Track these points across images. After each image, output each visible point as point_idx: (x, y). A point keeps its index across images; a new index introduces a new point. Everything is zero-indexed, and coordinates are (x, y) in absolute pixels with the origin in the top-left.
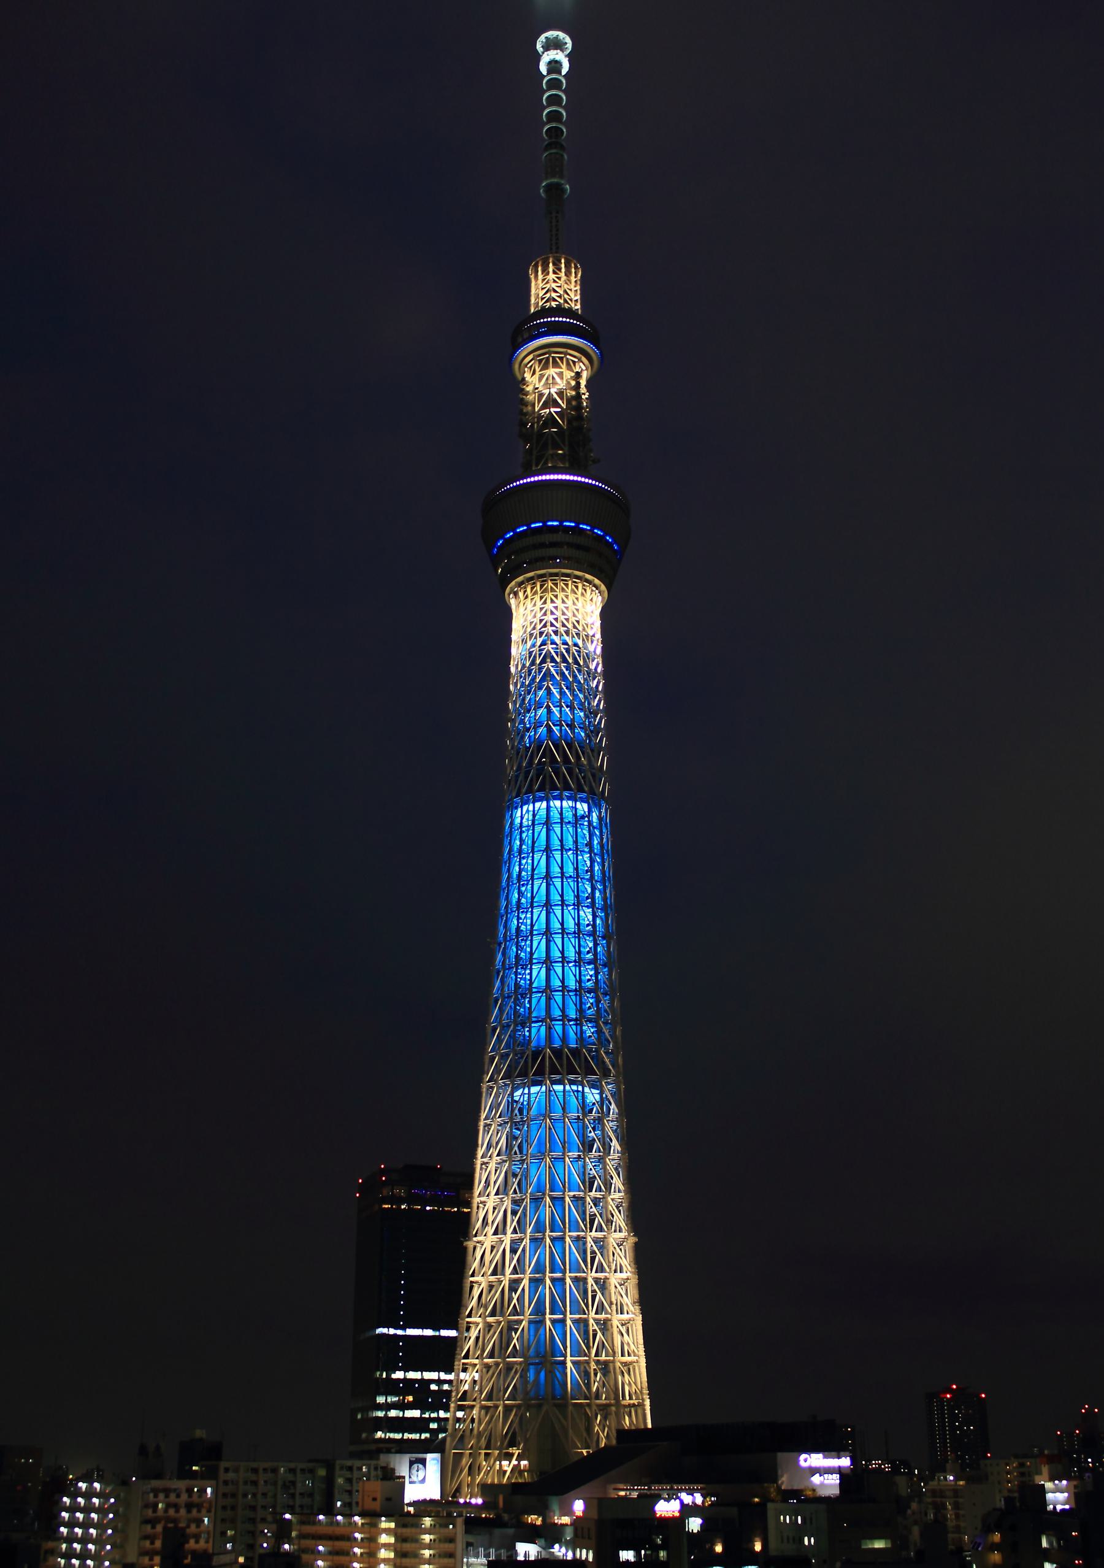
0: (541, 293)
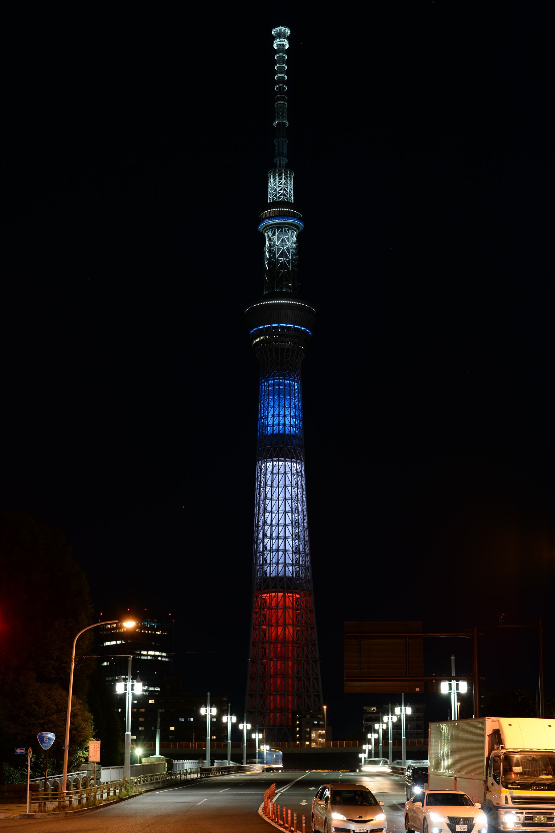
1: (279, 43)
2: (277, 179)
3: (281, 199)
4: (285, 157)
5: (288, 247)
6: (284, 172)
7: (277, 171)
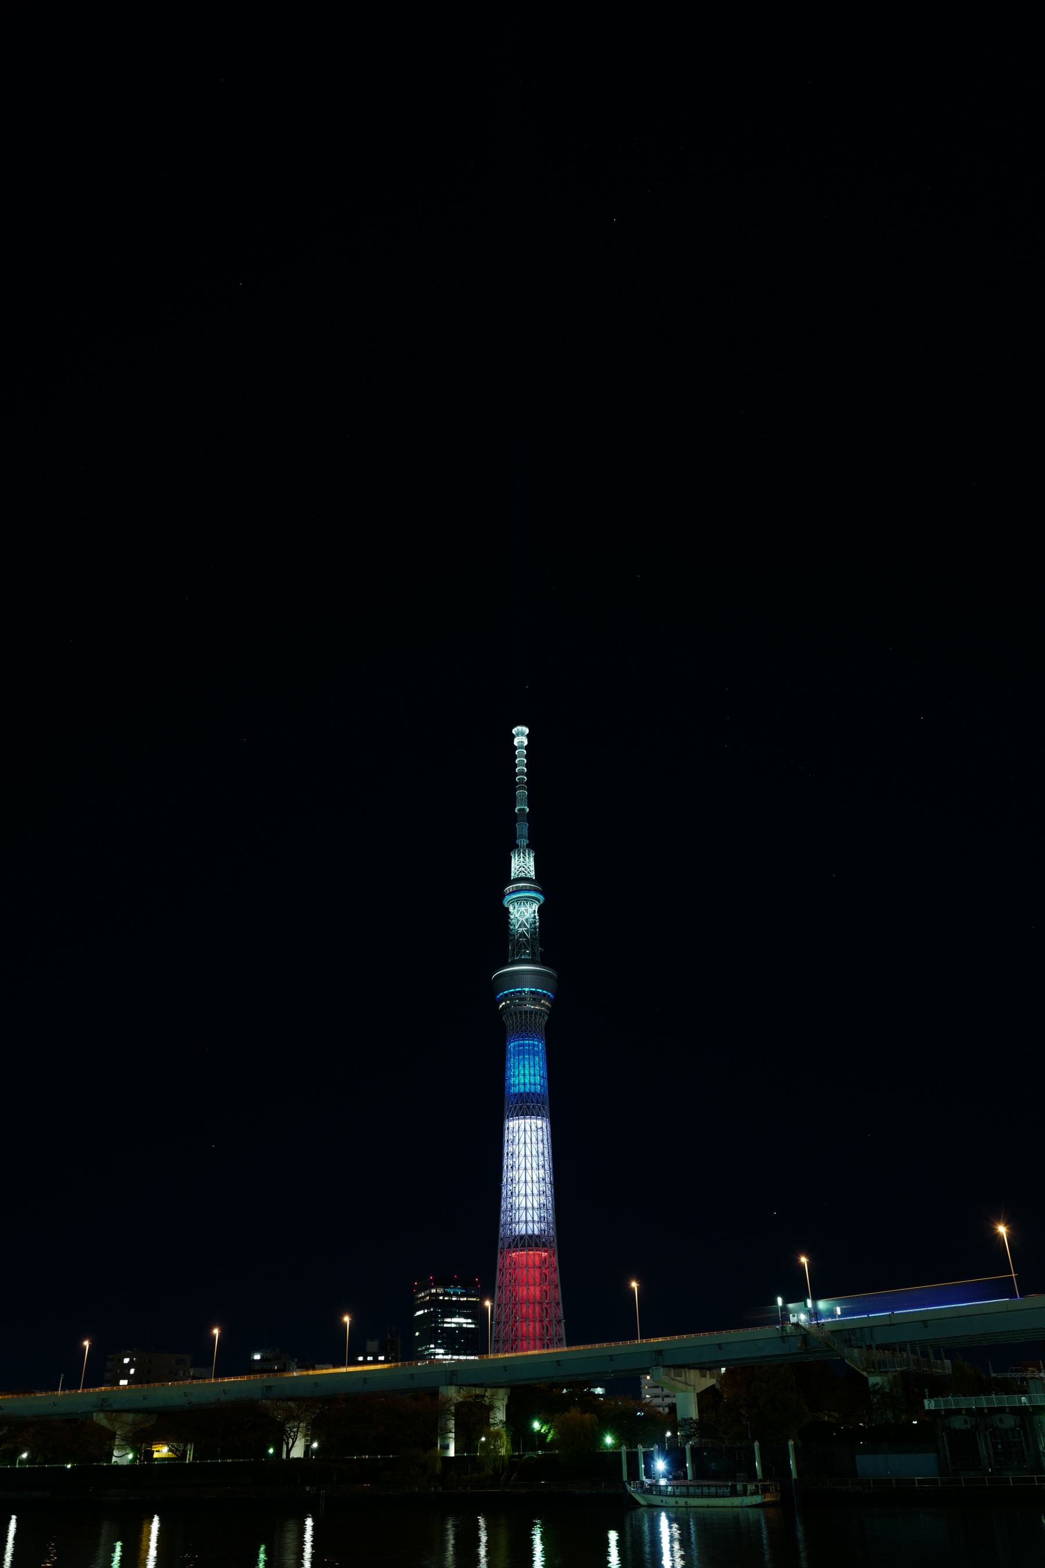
1: (518, 741)
4: (525, 838)
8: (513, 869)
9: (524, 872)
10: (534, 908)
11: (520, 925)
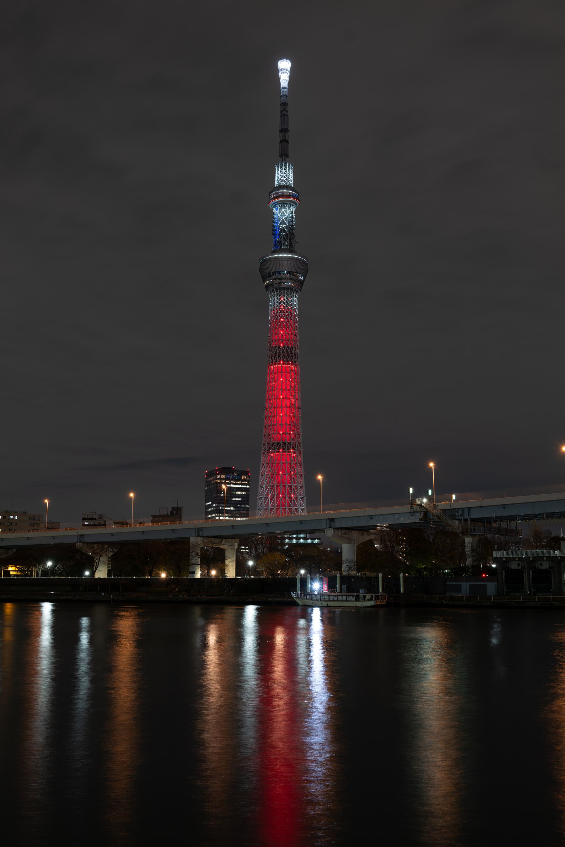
0: (280, 177)
2: (279, 170)
3: (281, 184)
5: (285, 217)
6: (284, 164)
7: (279, 164)
8: (276, 179)
9: (285, 181)
10: (292, 210)
11: (281, 222)
